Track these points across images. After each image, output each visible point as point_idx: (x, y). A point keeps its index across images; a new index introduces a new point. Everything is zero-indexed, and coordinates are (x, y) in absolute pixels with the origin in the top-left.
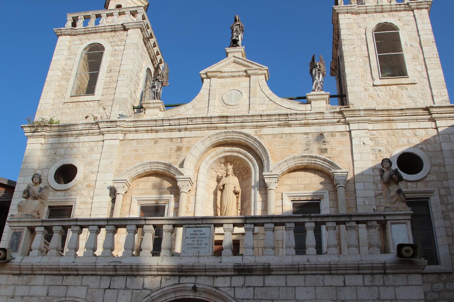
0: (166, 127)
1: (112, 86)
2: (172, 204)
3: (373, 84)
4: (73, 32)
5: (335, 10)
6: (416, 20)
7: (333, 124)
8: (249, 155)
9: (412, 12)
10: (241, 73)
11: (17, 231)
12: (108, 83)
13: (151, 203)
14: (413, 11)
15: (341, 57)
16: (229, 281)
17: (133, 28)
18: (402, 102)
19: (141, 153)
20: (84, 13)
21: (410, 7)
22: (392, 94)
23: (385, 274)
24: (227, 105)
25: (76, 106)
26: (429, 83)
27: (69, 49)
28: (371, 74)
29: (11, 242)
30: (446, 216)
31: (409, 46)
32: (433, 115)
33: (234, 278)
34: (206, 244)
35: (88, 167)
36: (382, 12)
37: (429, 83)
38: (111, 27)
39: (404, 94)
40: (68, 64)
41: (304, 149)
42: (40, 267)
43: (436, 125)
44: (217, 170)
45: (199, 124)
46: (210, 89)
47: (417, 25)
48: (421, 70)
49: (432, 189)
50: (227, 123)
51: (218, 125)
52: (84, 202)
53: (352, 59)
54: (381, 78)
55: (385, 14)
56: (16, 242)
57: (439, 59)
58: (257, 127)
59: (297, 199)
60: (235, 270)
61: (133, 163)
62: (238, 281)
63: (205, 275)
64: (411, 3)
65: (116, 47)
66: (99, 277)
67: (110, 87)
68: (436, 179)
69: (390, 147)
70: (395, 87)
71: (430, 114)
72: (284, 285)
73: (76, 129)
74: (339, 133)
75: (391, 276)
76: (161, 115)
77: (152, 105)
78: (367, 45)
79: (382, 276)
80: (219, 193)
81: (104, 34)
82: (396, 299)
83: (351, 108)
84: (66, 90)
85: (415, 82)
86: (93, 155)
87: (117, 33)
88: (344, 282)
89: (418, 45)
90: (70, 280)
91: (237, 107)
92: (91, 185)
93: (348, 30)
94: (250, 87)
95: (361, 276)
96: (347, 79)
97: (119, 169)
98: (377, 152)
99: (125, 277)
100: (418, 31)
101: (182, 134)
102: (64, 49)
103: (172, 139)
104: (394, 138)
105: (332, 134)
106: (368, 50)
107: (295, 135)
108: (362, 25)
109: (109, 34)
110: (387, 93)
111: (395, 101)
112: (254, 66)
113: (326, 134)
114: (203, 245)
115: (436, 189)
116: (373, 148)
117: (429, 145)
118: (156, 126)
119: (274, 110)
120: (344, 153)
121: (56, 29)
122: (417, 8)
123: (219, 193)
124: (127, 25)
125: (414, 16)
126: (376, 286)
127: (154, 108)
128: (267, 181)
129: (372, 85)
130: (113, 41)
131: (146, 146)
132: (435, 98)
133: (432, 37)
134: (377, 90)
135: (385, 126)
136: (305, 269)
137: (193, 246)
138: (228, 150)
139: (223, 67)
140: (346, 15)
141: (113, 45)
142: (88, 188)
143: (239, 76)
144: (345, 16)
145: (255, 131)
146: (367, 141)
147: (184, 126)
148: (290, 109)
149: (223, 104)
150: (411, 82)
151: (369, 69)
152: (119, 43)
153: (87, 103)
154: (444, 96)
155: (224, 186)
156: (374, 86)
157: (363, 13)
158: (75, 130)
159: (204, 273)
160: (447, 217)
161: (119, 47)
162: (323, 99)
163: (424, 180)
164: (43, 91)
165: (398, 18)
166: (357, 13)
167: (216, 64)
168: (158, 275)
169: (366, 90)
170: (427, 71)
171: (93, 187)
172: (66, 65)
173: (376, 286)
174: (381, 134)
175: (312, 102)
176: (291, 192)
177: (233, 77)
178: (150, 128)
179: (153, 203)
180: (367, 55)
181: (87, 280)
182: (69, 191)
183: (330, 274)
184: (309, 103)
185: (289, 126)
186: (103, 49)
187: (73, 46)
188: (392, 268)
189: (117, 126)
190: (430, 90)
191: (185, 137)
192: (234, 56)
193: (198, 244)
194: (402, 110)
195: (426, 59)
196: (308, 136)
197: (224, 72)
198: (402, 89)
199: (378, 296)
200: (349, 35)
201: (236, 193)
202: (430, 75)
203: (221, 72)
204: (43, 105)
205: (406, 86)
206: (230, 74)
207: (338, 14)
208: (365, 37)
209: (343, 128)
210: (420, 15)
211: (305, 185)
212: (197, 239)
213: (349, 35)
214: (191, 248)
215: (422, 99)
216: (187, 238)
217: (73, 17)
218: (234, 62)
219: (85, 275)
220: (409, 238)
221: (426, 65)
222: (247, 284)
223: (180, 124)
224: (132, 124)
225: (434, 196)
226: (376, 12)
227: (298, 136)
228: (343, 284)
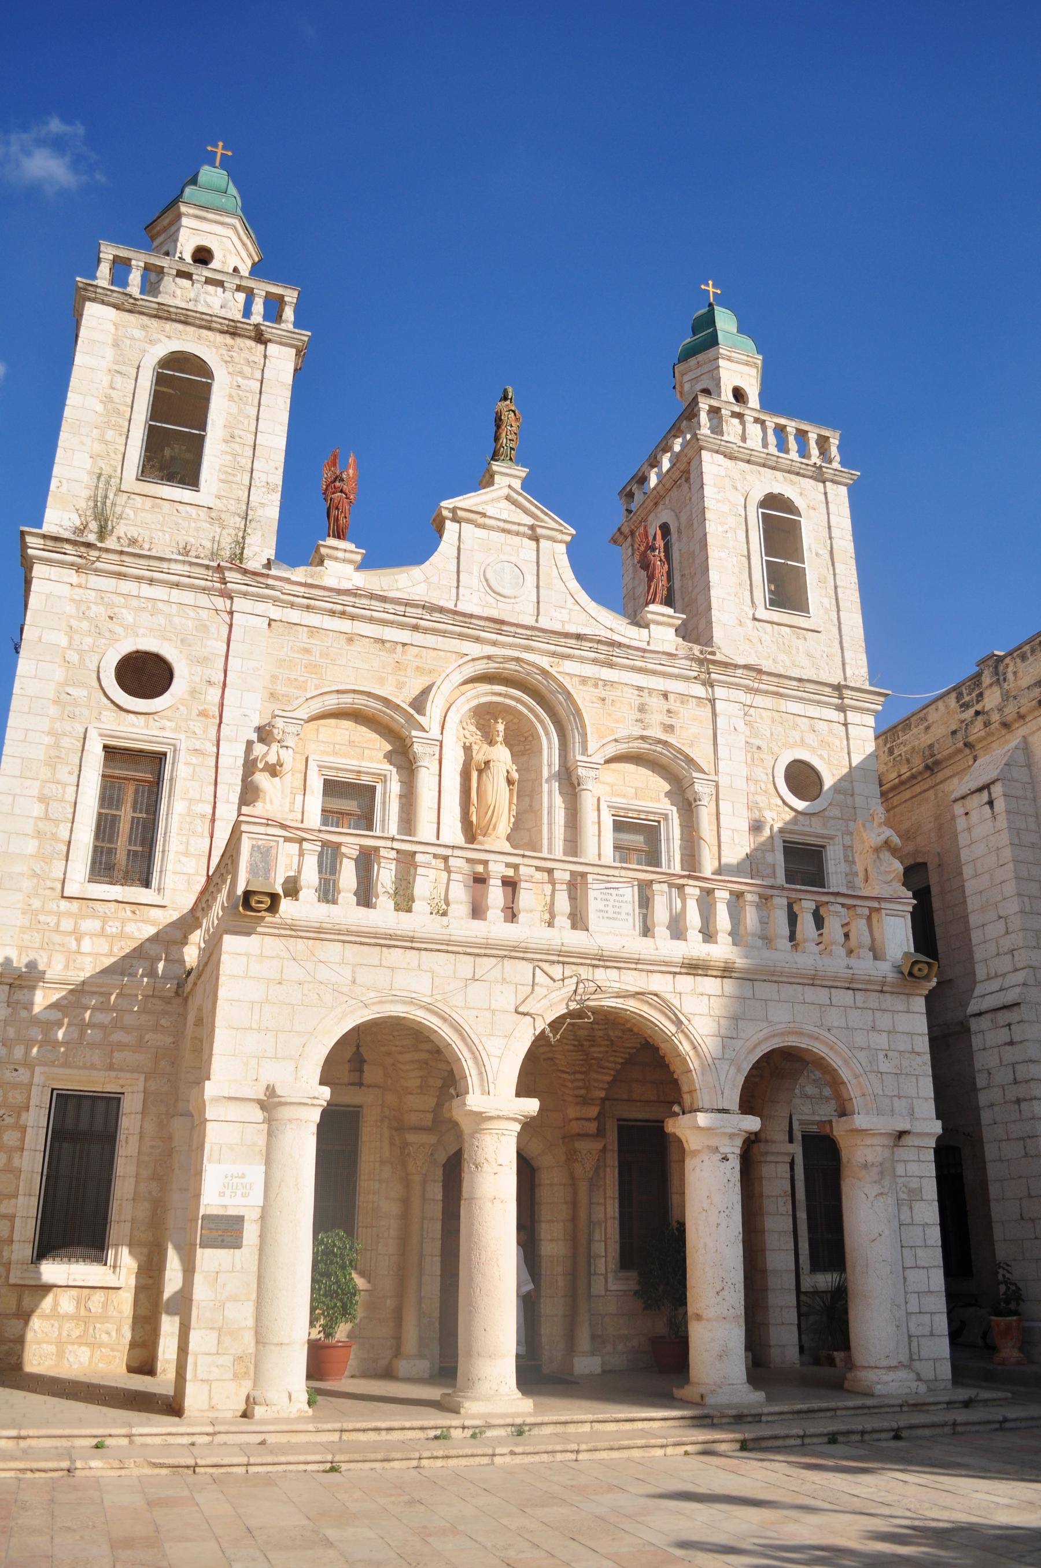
0: (375, 614)
1: (238, 479)
2: (395, 787)
3: (754, 614)
4: (115, 298)
5: (698, 439)
6: (827, 503)
7: (687, 679)
8: (539, 710)
9: (821, 485)
10: (522, 529)
11: (260, 843)
12: (229, 470)
13: (347, 776)
14: (824, 482)
15: (679, 531)
17: (281, 344)
18: (797, 664)
19: (318, 659)
20: (147, 256)
21: (822, 474)
22: (781, 643)
23: (882, 991)
24: (494, 592)
25: (153, 507)
26: (841, 636)
27: (116, 345)
28: (752, 593)
29: (251, 865)
30: (850, 882)
31: (814, 553)
32: (847, 701)
33: (678, 976)
34: (627, 914)
35: (199, 668)
36: (774, 468)
37: (841, 636)
38: (226, 322)
39: (801, 648)
40: (118, 386)
41: (635, 717)
42: (337, 927)
43: (846, 719)
44: (465, 726)
45: (444, 623)
46: (459, 546)
47: (828, 514)
48: (828, 607)
49: (834, 833)
50: (500, 634)
51: (483, 634)
52: (197, 750)
53: (723, 555)
54: (768, 606)
55: (779, 474)
56: (263, 867)
57: (858, 593)
58: (554, 654)
59: (622, 814)
60: (683, 965)
61: (303, 679)
62: (685, 982)
63: (635, 969)
64: (827, 468)
65: (239, 379)
67: (234, 479)
68: (839, 815)
69: (775, 743)
70: (787, 629)
71: (841, 698)
72: (751, 996)
73: (164, 570)
74: (694, 699)
75: (888, 995)
76: (360, 580)
77: (340, 554)
78: (747, 531)
79: (877, 993)
80: (475, 775)
81: (205, 332)
83: (718, 657)
84: (120, 457)
85: (819, 630)
86: (209, 643)
87: (239, 341)
89: (828, 556)
91: (513, 601)
92: (211, 713)
93: (716, 490)
94: (538, 563)
95: (851, 992)
96: (713, 593)
97: (271, 687)
98: (755, 750)
100: (829, 528)
101: (405, 636)
102: (104, 343)
103: (383, 642)
104: (781, 729)
105: (683, 697)
106: (748, 543)
107: (620, 686)
108: (739, 487)
109: (220, 338)
110: (774, 640)
111: (786, 658)
112: (551, 521)
113: (672, 695)
114: (623, 916)
115: (839, 834)
116: (748, 740)
117: (832, 753)
118: (354, 607)
119: (584, 625)
120: (701, 740)
121: (85, 281)
122: (832, 481)
123: (475, 775)
124: (269, 330)
125: (826, 494)
126: (870, 1009)
127: (344, 560)
128: (581, 772)
129: (751, 616)
130: (229, 359)
131: (326, 644)
132: (848, 667)
133: (850, 547)
134: (760, 629)
136: (781, 974)
137: (606, 915)
138: (500, 691)
139: (485, 503)
140: (715, 455)
141: (231, 370)
142: (203, 719)
143: (517, 534)
144: (712, 456)
145: (549, 662)
146: (740, 725)
147: (414, 621)
148: (611, 629)
149: (488, 589)
150: (813, 628)
151: (749, 582)
152: (247, 370)
153: (181, 507)
154: (862, 667)
155: (487, 763)
156: (755, 619)
157: (742, 460)
158: (162, 572)
159: (633, 966)
160: (850, 885)
161: (246, 382)
162: (670, 625)
163: (822, 814)
164: (60, 443)
165: (799, 491)
166: (731, 457)
167: (473, 494)
168: (559, 962)
169: (741, 624)
170: (838, 611)
171: (214, 717)
172: (114, 388)
173: (870, 1009)
174: (761, 717)
175: (652, 626)
176: (614, 799)
177: (504, 531)
178: (339, 608)
179: (351, 777)
180: (746, 553)
181: (429, 959)
182: (156, 718)
183: (812, 985)
184: (647, 626)
185: (611, 665)
186: (210, 374)
187: (128, 342)
188: (893, 985)
189: (268, 586)
190: (840, 651)
191: (412, 645)
192: (509, 486)
193: (615, 913)
194: (800, 680)
195: (838, 589)
196: (641, 693)
197: (490, 517)
198: (798, 638)
199: (872, 1024)
200: (718, 501)
201: (510, 782)
202: (842, 621)
203: (484, 515)
204: (64, 481)
205: (805, 632)
206: (501, 524)
207: (701, 448)
208: (743, 514)
209: (699, 690)
210: (836, 495)
211: (636, 789)
212: (611, 903)
213: (718, 501)
214: (603, 918)
215: (828, 664)
216: (596, 899)
217: (115, 256)
218: (508, 498)
219: (426, 949)
220: (908, 940)
221: (837, 599)
222: (700, 990)
223: (406, 614)
224: (302, 589)
225: (834, 845)
226: (764, 465)
227: (625, 689)
228: (828, 1002)
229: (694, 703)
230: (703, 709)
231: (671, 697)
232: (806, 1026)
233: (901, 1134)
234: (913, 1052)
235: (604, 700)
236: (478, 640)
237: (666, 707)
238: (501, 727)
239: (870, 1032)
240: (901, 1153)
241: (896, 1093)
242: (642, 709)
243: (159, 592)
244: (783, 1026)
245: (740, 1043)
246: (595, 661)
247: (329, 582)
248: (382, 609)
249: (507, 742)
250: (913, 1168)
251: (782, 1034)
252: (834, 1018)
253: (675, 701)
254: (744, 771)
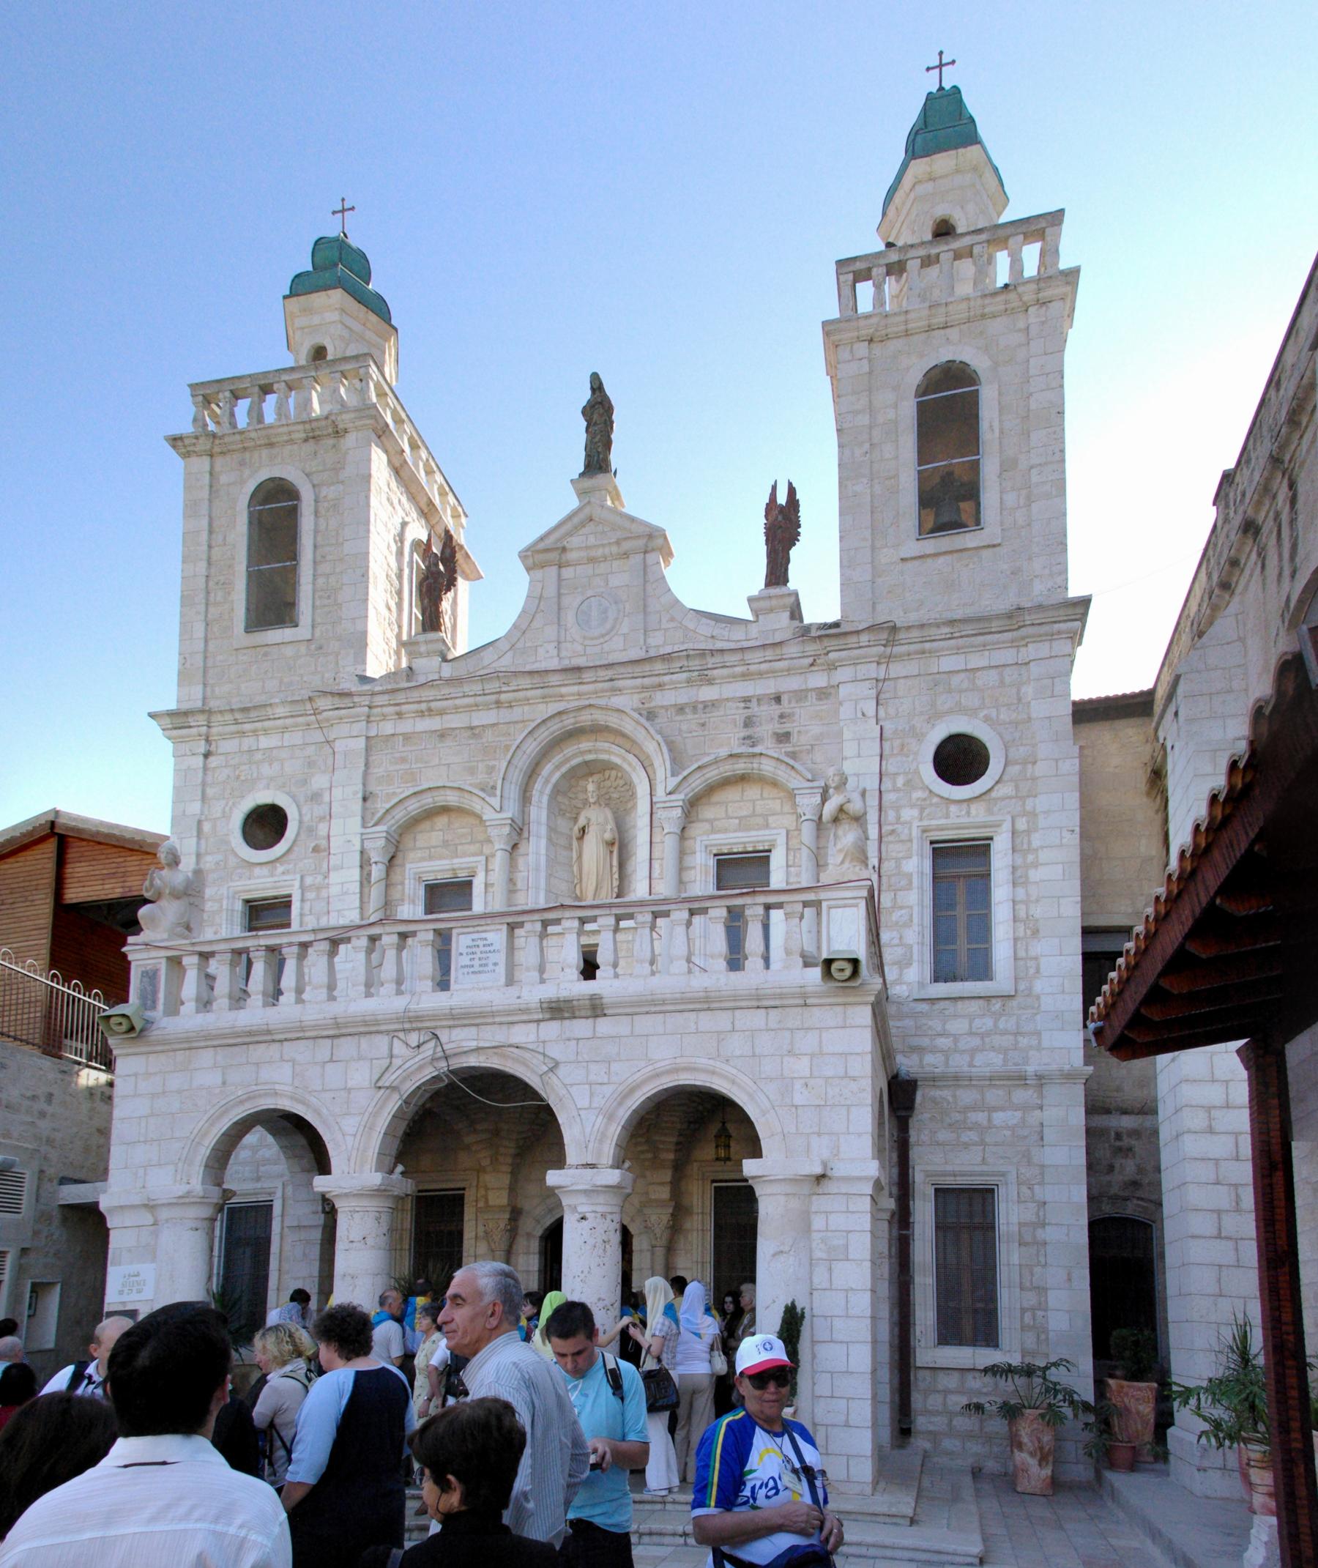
0: (458, 702)
16: (535, 1031)
41: (742, 735)
51: (564, 690)
62: (552, 1029)
66: (310, 1043)
82: (821, 1054)
88: (733, 1023)
90: (259, 1052)
99: (357, 1037)
105: (800, 695)
127: (428, 654)
136: (664, 1002)
168: (414, 1030)
183: (709, 1009)
185: (710, 682)
196: (748, 704)
219: (286, 1040)
229: (814, 697)
230: (825, 702)
231: (785, 698)
232: (698, 1060)
233: (821, 1178)
234: (846, 1076)
235: (703, 725)
237: (778, 712)
239: (786, 1059)
240: (819, 1203)
241: (816, 1129)
242: (748, 723)
244: (667, 1062)
245: (612, 1088)
248: (461, 695)
250: (838, 1221)
251: (668, 1072)
252: (736, 1045)
253: (790, 702)
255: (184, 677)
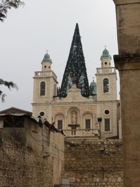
7: (93, 104)
55: (106, 76)
105: (93, 106)
135: (103, 104)
146: (99, 107)
166: (100, 75)
236: (71, 104)
238: (74, 113)
243: (43, 106)
246: (83, 104)
247: (57, 102)
249: (75, 113)
254: (100, 112)
255: (34, 99)
